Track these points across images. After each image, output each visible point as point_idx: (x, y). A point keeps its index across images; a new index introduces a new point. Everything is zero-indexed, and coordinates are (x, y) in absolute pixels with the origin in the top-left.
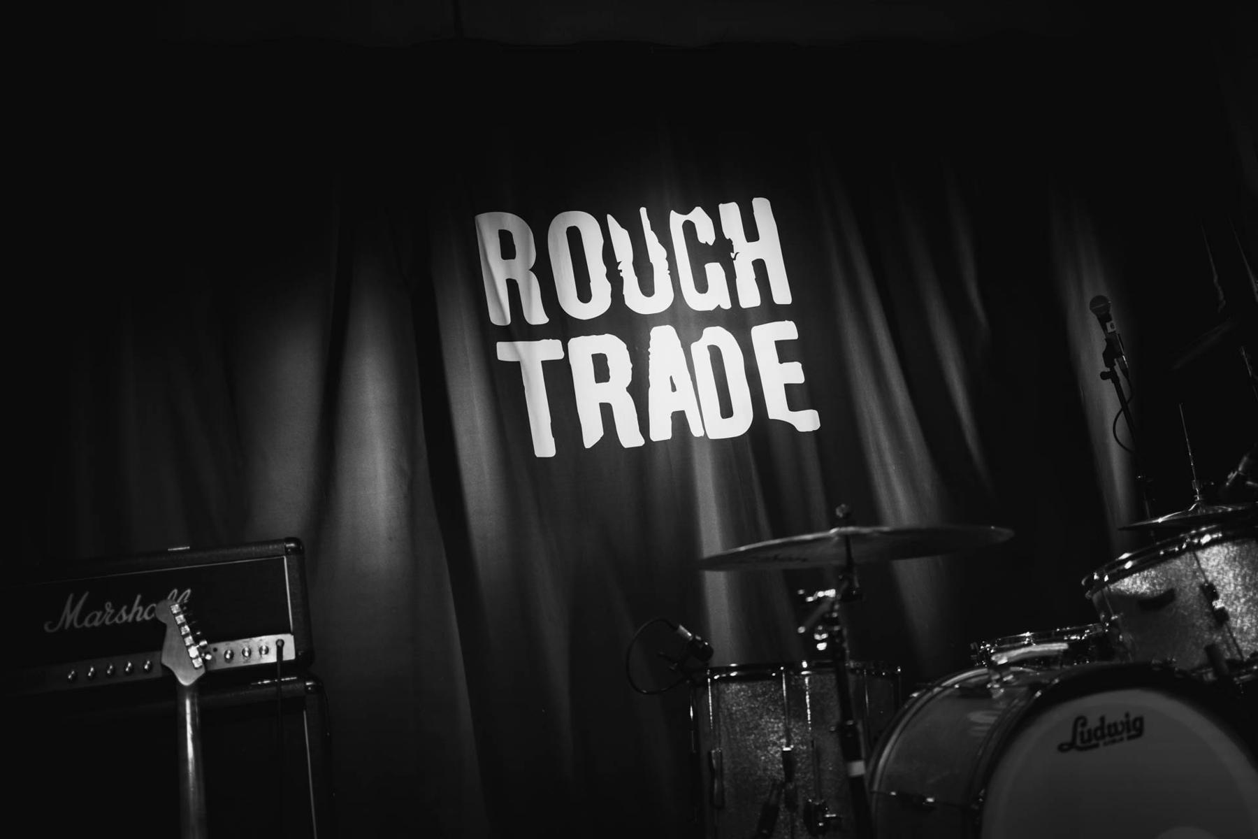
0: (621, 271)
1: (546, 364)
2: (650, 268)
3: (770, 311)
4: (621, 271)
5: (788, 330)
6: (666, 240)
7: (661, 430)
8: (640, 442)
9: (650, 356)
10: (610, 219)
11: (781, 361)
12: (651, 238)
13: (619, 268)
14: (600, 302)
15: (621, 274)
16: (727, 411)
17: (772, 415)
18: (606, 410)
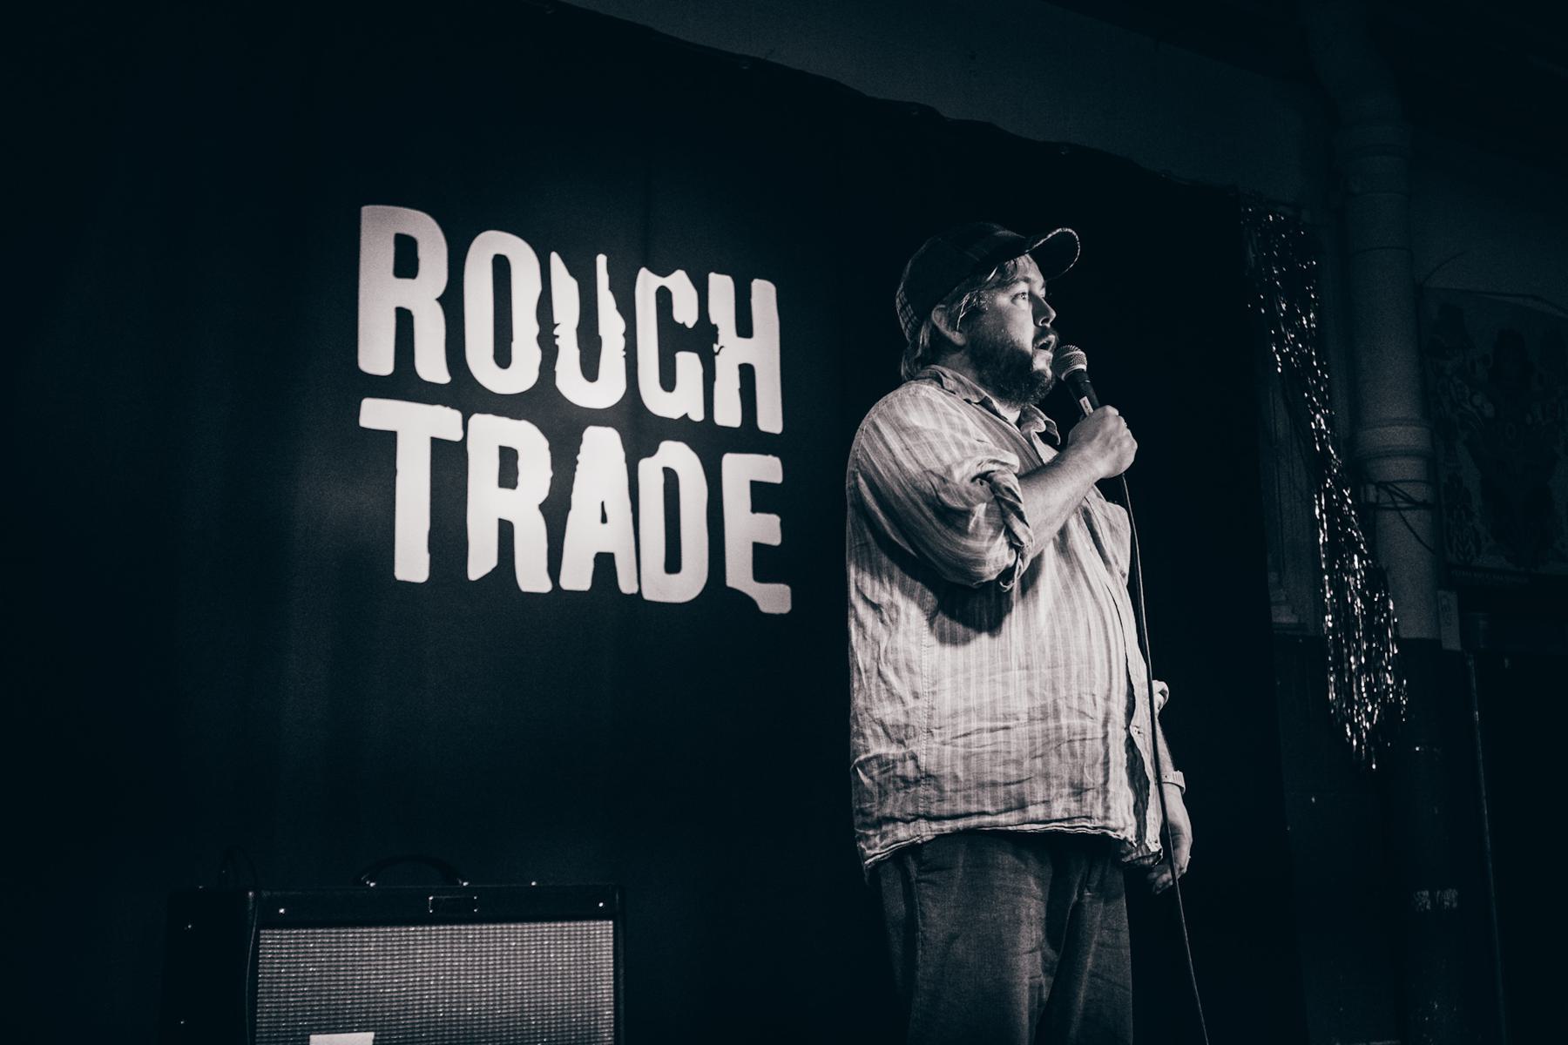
0: (557, 336)
1: (436, 443)
2: (598, 342)
3: (748, 438)
4: (557, 336)
5: (769, 469)
6: (627, 308)
7: (576, 577)
8: (545, 586)
9: (578, 467)
11: (755, 509)
12: (606, 301)
13: (556, 332)
14: (520, 377)
15: (557, 342)
16: (673, 563)
17: (730, 583)
18: (506, 531)
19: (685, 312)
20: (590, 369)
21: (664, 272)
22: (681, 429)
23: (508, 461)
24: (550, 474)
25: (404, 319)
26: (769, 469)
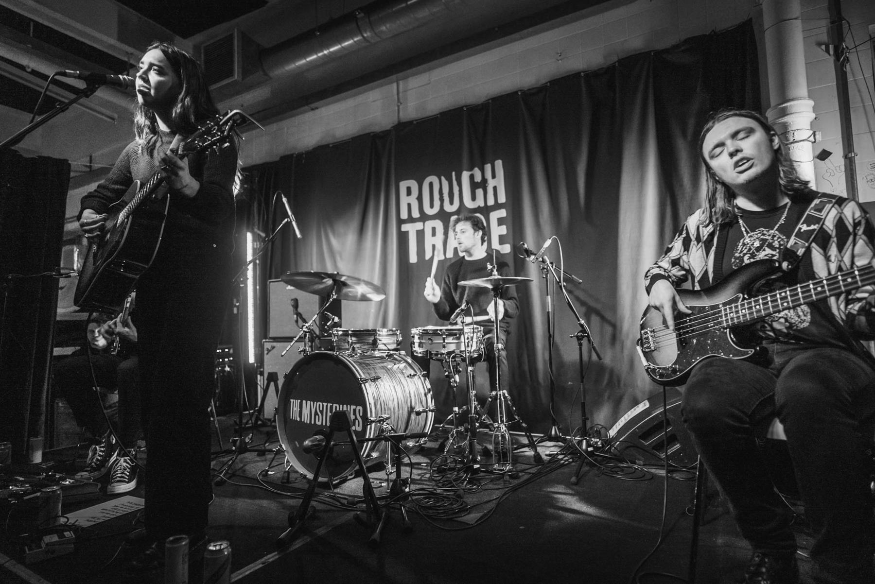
1: (417, 231)
3: (497, 206)
5: (503, 213)
7: (450, 254)
10: (443, 178)
13: (444, 195)
14: (436, 209)
15: (444, 198)
17: (493, 247)
19: (478, 178)
20: (451, 203)
21: (471, 169)
22: (478, 210)
23: (434, 229)
24: (443, 231)
25: (409, 205)
26: (503, 213)
